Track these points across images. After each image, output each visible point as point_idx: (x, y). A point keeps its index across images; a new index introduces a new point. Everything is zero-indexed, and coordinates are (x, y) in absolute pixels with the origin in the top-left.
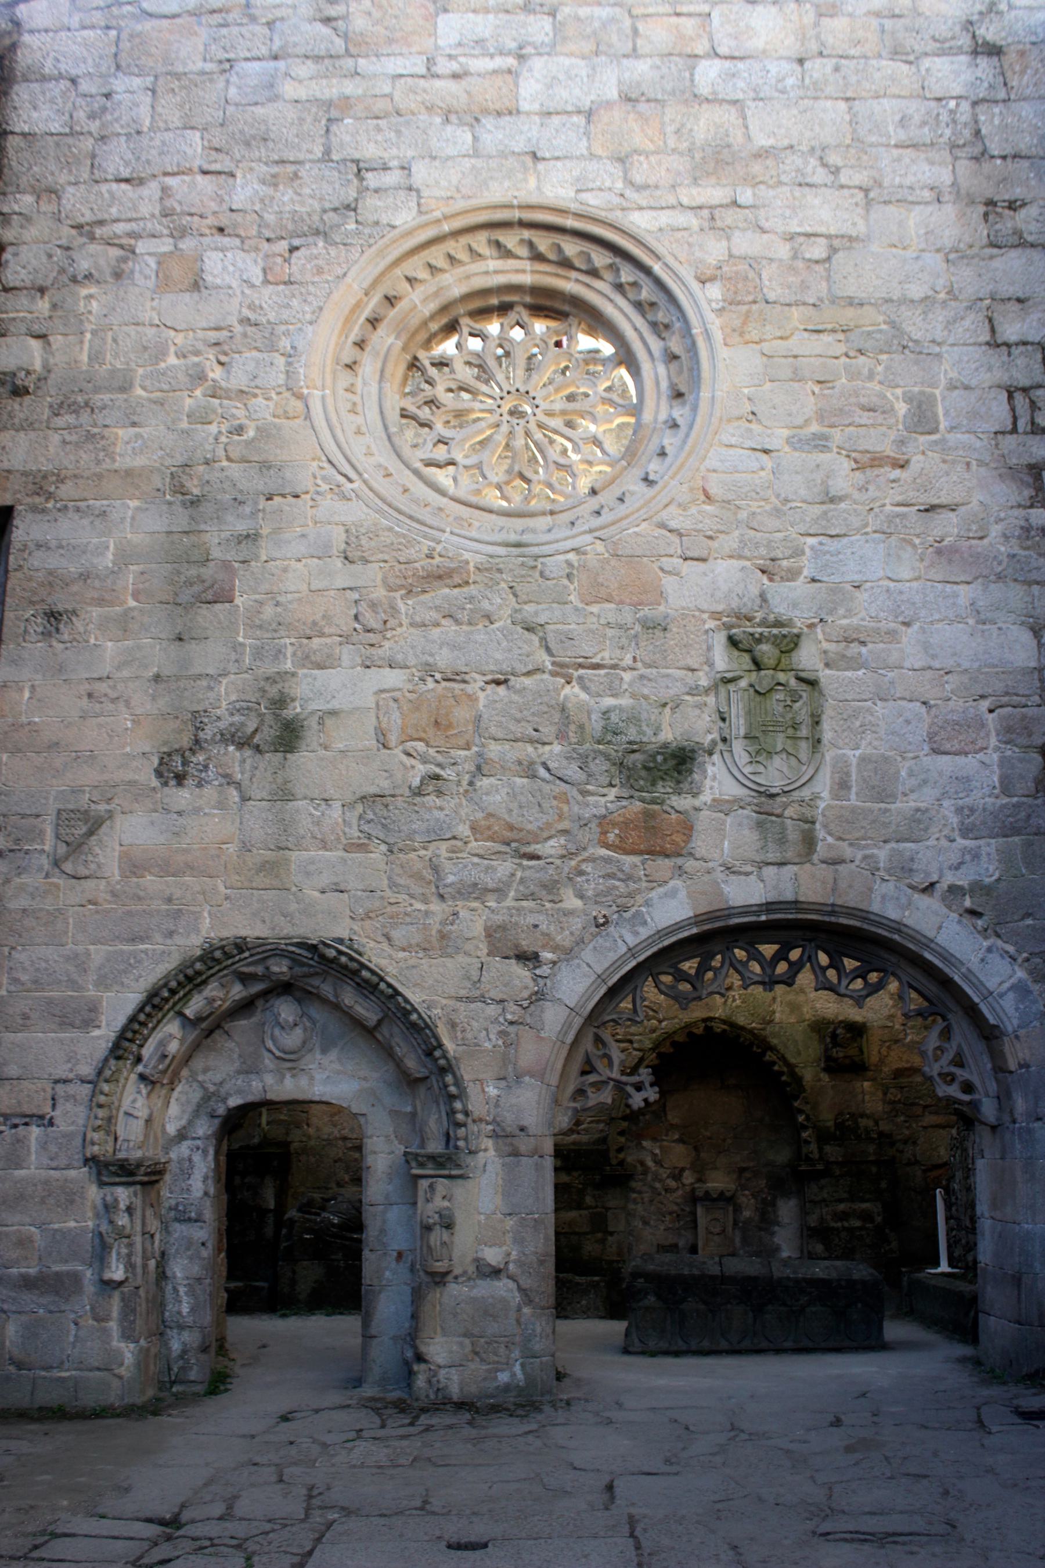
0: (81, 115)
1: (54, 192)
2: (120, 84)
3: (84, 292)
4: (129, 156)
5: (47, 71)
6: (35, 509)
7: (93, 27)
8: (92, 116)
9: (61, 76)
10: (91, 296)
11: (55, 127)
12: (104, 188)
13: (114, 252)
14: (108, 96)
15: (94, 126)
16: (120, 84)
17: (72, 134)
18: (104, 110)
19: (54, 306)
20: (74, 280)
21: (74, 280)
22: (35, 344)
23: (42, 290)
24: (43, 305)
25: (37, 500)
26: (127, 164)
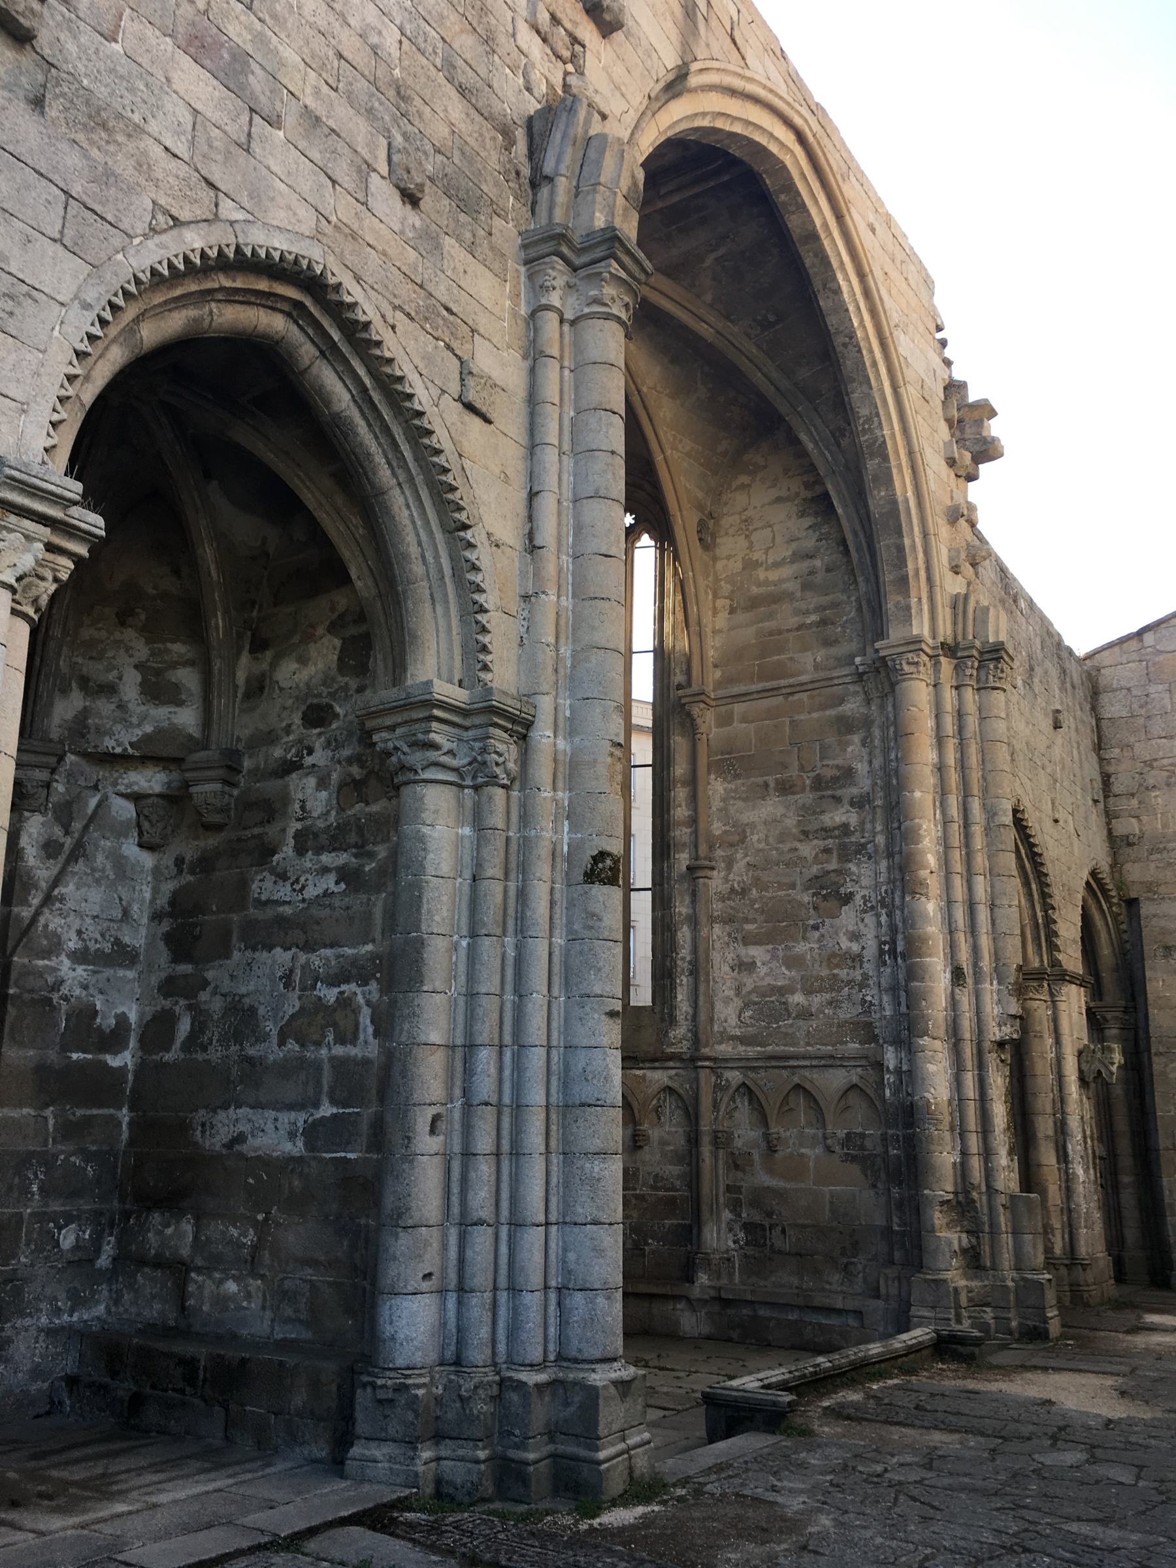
0: (1135, 706)
1: (1130, 746)
2: (1152, 689)
3: (1153, 794)
4: (1163, 725)
5: (1114, 686)
6: (1148, 899)
7: (1134, 661)
8: (1141, 707)
9: (1122, 689)
10: (1156, 797)
11: (1124, 714)
12: (1154, 742)
13: (1165, 774)
14: (1147, 695)
15: (1143, 711)
16: (1152, 689)
17: (1132, 716)
18: (1147, 703)
19: (1140, 803)
20: (1147, 788)
21: (1147, 788)
22: (1134, 820)
23: (1133, 795)
24: (1134, 802)
25: (1150, 895)
26: (1163, 729)
